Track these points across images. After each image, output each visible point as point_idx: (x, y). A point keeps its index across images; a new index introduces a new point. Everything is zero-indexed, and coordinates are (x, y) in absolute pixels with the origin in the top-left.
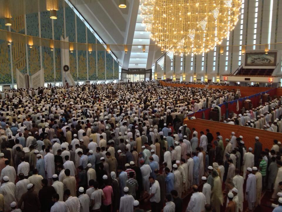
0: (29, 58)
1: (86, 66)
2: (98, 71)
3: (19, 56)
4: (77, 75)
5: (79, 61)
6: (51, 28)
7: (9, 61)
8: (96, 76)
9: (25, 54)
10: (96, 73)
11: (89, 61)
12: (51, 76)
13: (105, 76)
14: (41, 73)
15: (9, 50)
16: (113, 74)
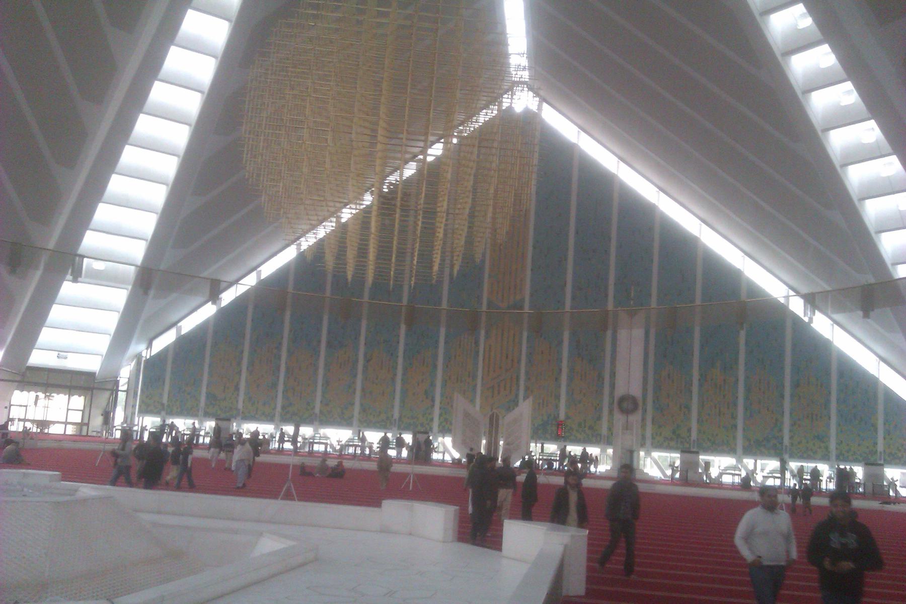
0: (527, 373)
1: (735, 405)
2: (793, 424)
3: (501, 368)
4: (689, 430)
5: (701, 385)
6: (606, 288)
7: (474, 377)
8: (782, 443)
9: (519, 361)
10: (781, 430)
11: (748, 390)
12: (591, 428)
13: (827, 448)
14: (525, 408)
15: (477, 352)
16: (875, 444)
